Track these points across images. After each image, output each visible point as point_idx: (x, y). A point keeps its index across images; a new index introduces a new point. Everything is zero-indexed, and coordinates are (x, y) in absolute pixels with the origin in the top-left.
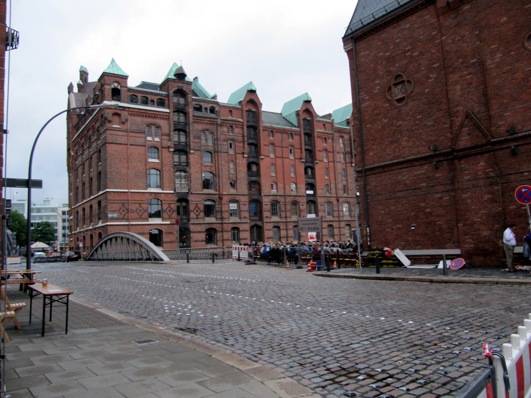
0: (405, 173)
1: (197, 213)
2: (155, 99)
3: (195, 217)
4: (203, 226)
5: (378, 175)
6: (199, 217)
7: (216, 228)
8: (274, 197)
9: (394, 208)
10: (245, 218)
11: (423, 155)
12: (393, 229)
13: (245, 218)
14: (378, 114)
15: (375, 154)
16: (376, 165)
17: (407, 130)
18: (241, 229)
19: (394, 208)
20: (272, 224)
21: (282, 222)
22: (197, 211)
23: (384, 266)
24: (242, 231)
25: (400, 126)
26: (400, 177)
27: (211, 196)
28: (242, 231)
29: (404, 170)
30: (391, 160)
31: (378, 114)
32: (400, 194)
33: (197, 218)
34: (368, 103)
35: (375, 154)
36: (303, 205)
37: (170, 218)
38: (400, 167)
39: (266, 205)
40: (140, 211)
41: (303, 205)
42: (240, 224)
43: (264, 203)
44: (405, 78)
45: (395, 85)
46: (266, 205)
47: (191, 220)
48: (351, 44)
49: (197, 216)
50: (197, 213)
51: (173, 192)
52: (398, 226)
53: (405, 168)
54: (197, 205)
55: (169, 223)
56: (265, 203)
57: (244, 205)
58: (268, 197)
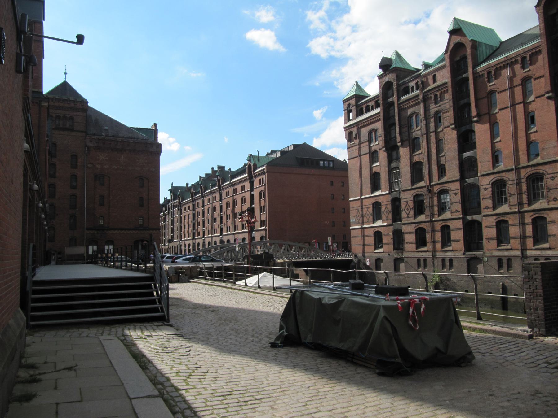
1: (408, 212)
2: (372, 103)
3: (406, 216)
4: (413, 225)
6: (410, 216)
7: (425, 228)
8: (497, 175)
10: (457, 211)
13: (457, 211)
18: (452, 227)
20: (495, 217)
21: (512, 213)
22: (408, 209)
24: (454, 230)
27: (420, 190)
28: (454, 230)
33: (408, 217)
37: (387, 220)
39: (486, 189)
40: (368, 215)
42: (451, 222)
43: (481, 187)
46: (486, 189)
47: (403, 220)
49: (408, 215)
50: (408, 212)
51: (387, 192)
54: (407, 202)
55: (385, 224)
56: (484, 187)
57: (456, 194)
58: (487, 177)
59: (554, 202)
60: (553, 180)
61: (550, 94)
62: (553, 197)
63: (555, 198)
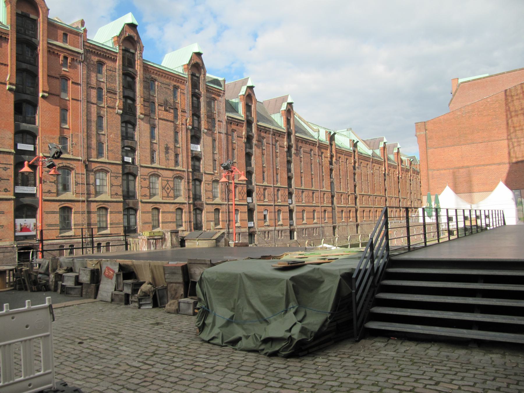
36: (5, 169)
41: (5, 169)
59: (4, 193)
60: (5, 170)
61: (14, 87)
62: (4, 188)
63: (6, 189)
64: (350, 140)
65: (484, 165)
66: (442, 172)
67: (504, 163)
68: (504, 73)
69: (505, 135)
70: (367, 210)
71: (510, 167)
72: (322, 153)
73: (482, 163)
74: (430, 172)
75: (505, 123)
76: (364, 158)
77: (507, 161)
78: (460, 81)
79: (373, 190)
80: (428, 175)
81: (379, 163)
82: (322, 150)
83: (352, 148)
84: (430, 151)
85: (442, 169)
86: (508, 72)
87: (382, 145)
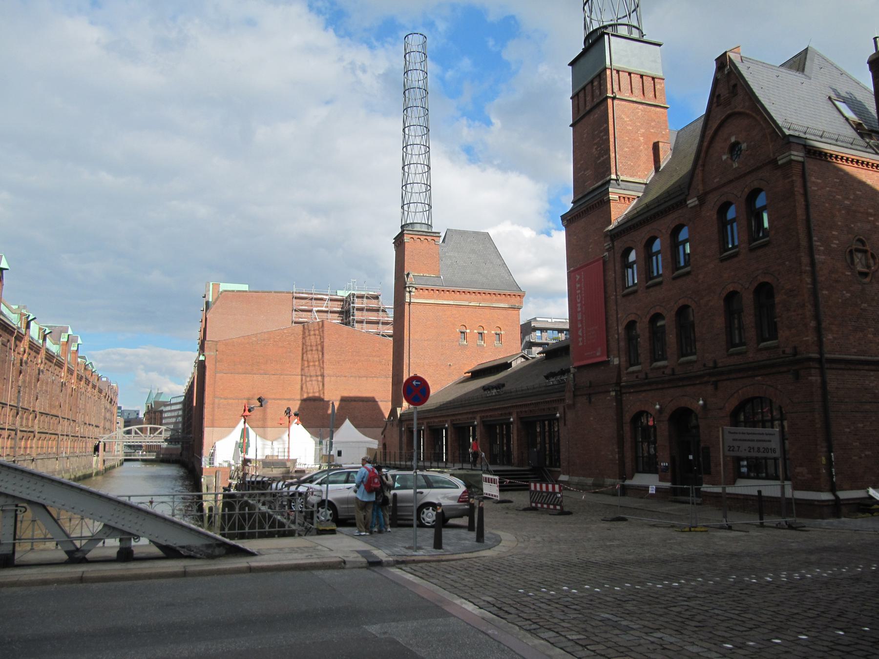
0: (873, 378)
5: (840, 372)
9: (862, 425)
11: (849, 357)
12: (861, 458)
14: (837, 281)
15: (835, 338)
16: (837, 356)
17: (874, 320)
19: (862, 425)
23: (875, 514)
25: (864, 310)
26: (867, 382)
29: (872, 373)
30: (856, 354)
31: (837, 281)
32: (868, 407)
34: (823, 257)
35: (835, 338)
38: (867, 367)
44: (868, 248)
45: (858, 250)
48: (802, 154)
52: (867, 453)
53: (872, 370)
64: (40, 329)
65: (274, 399)
66: (231, 401)
67: (294, 400)
68: (270, 292)
69: (299, 370)
70: (43, 436)
71: (301, 404)
72: (16, 346)
73: (273, 396)
74: (217, 400)
75: (300, 358)
76: (50, 357)
77: (299, 397)
78: (224, 286)
79: (51, 406)
80: (213, 404)
81: (60, 365)
82: (18, 342)
83: (41, 341)
84: (218, 375)
85: (231, 398)
86: (275, 292)
87: (64, 339)
